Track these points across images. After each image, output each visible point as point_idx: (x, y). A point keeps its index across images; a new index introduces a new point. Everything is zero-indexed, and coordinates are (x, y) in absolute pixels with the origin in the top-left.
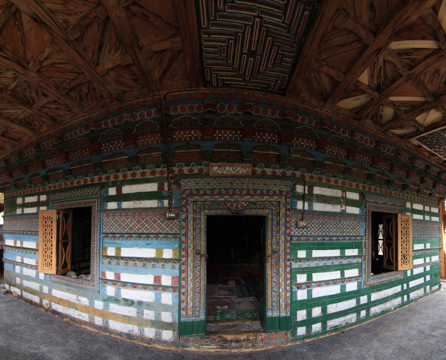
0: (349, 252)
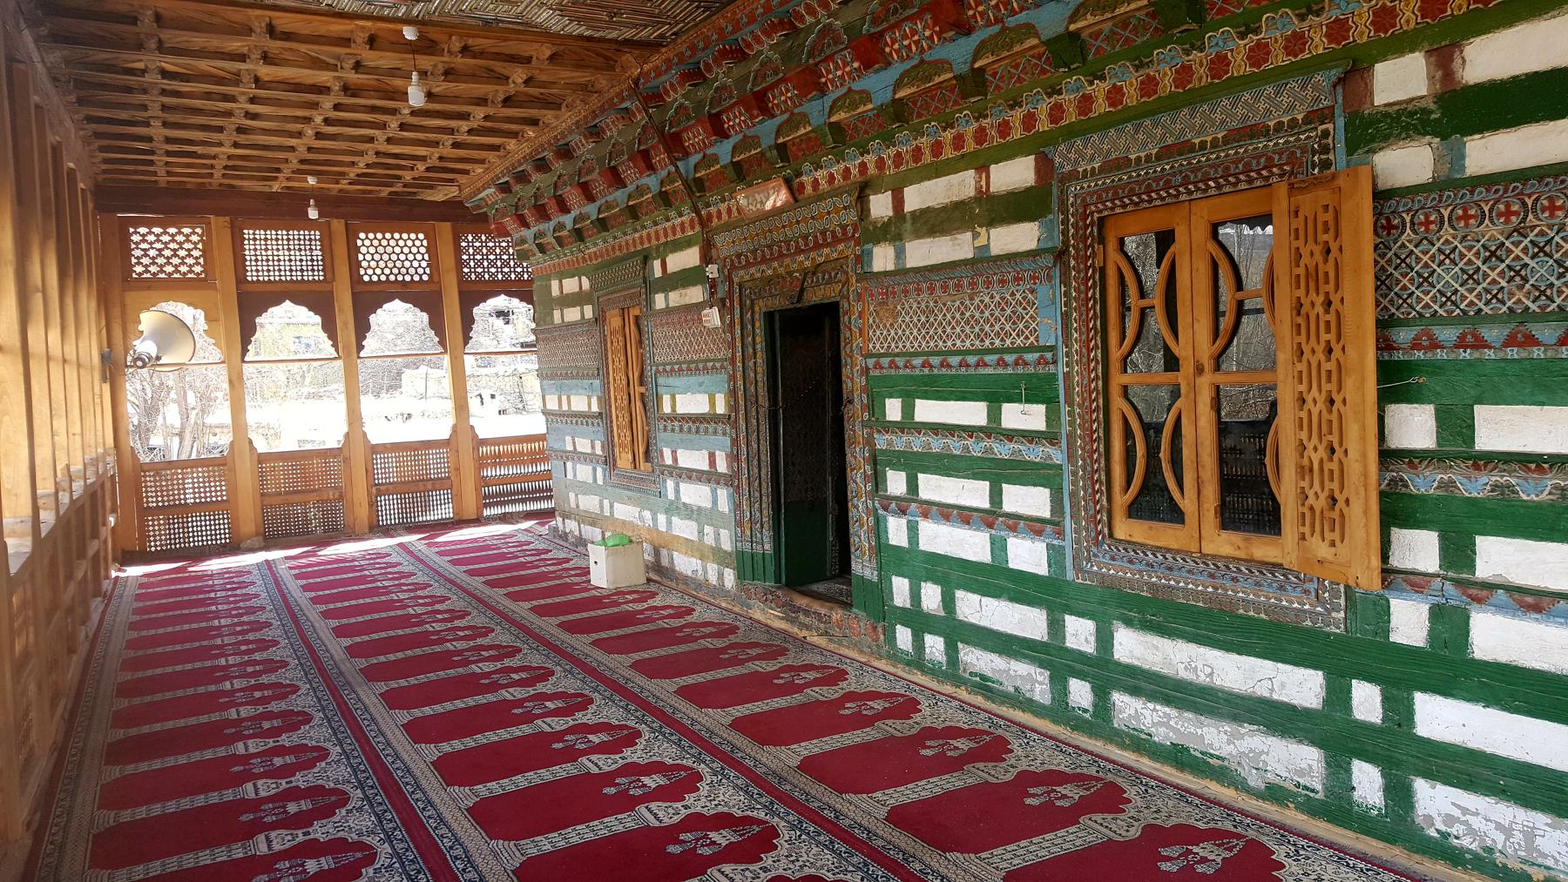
0: (1017, 416)
